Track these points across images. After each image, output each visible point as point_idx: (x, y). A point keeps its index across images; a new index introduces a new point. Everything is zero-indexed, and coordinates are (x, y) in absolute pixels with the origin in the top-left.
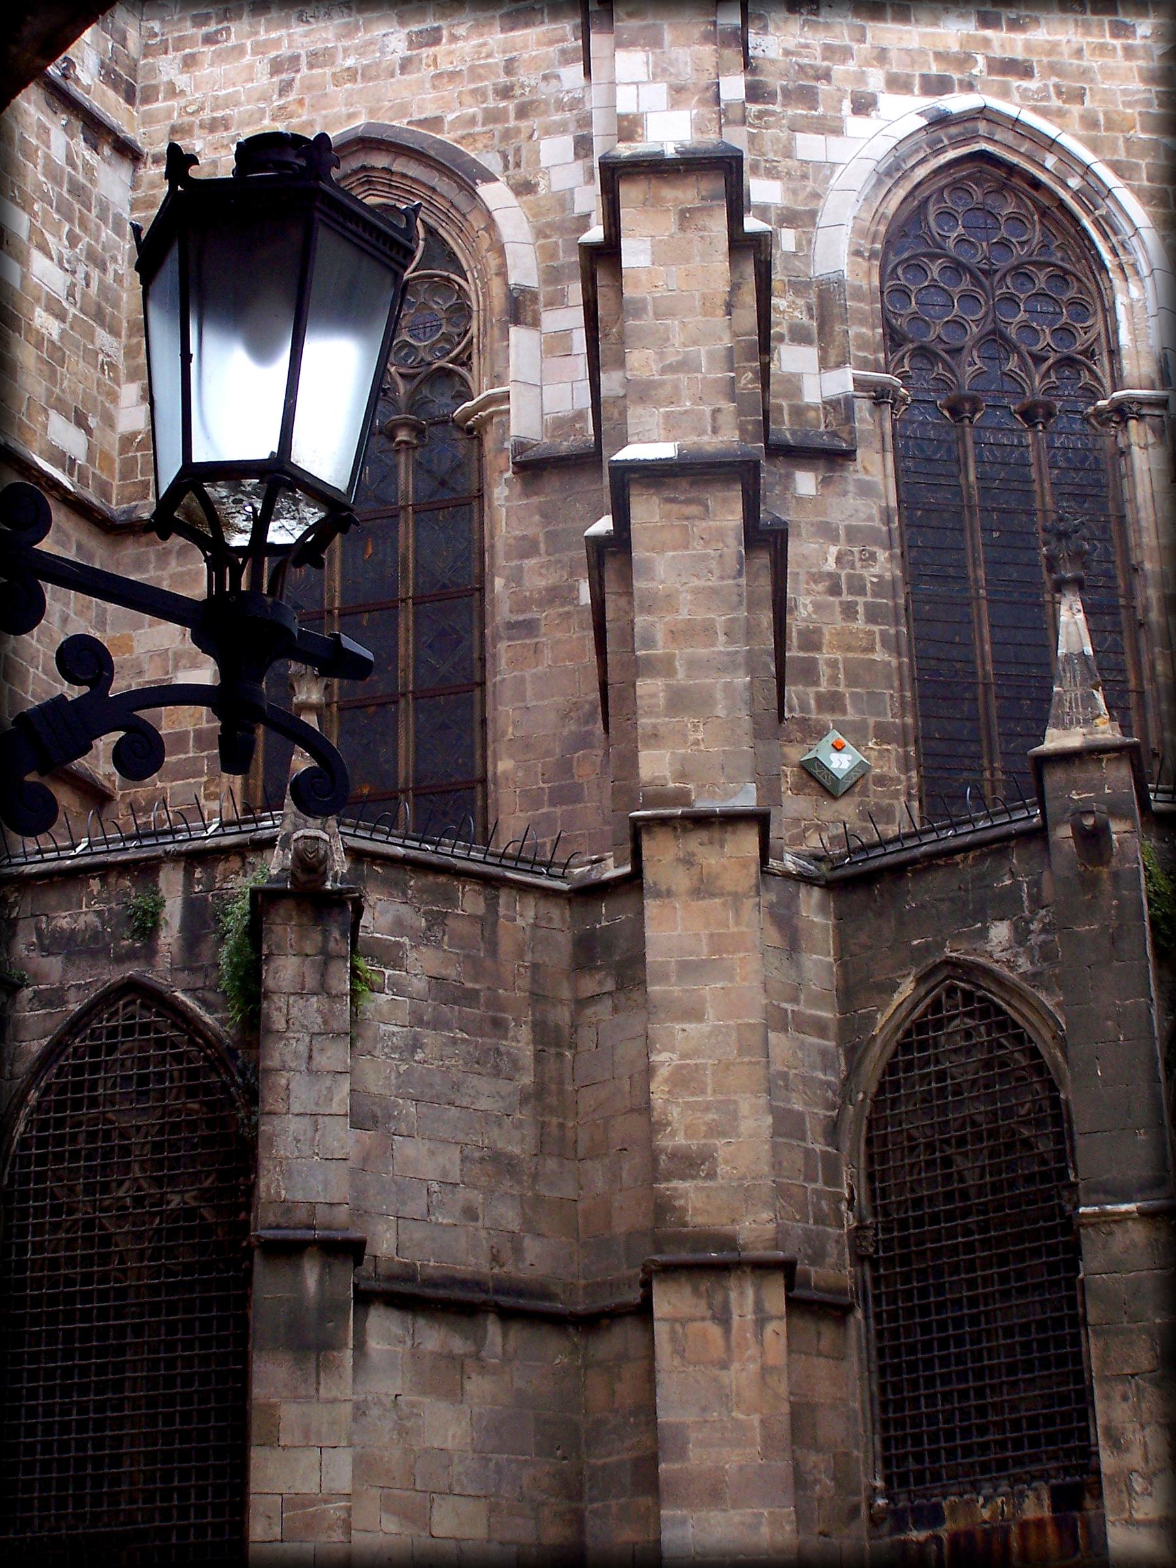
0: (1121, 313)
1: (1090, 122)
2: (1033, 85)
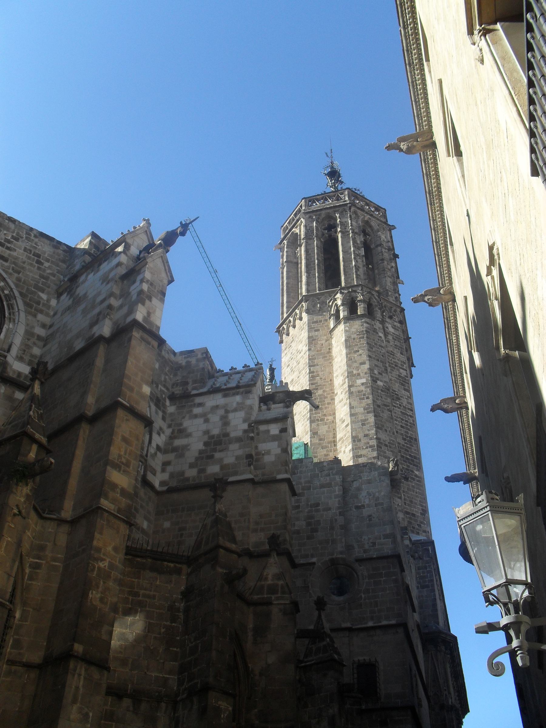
0: (4, 330)
1: (19, 280)
2: (6, 264)
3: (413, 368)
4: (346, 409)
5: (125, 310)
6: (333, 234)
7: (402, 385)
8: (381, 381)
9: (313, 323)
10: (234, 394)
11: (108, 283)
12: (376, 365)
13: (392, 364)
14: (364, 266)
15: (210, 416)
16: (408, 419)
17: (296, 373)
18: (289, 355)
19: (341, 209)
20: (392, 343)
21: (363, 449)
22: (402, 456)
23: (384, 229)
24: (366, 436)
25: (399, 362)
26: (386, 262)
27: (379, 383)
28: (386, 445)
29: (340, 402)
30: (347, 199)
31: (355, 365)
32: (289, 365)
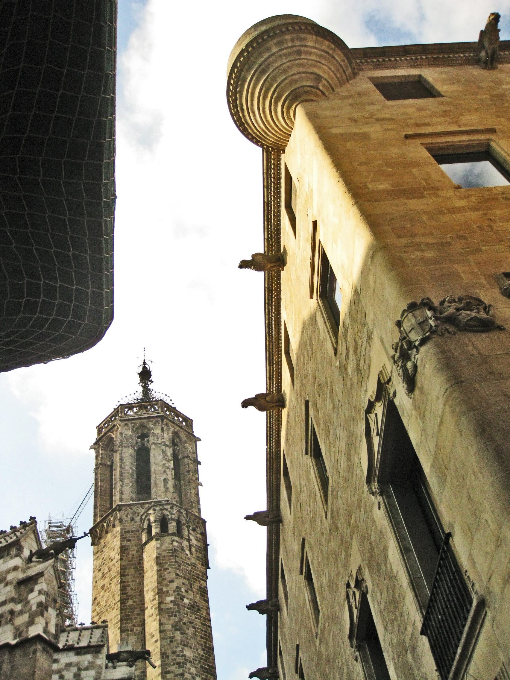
3: (208, 570)
4: (156, 624)
5: (25, 618)
6: (146, 443)
7: (203, 596)
8: (187, 598)
9: (126, 532)
10: (85, 653)
11: (6, 585)
12: (183, 583)
13: (194, 575)
14: (173, 479)
15: (64, 673)
16: (207, 629)
17: (108, 580)
18: (101, 560)
19: (154, 420)
20: (194, 555)
21: (171, 665)
22: (202, 667)
23: (190, 440)
24: (174, 652)
25: (200, 574)
26: (191, 474)
27: (186, 601)
28: (190, 662)
29: (150, 617)
30: (160, 410)
31: (165, 582)
32: (100, 570)
